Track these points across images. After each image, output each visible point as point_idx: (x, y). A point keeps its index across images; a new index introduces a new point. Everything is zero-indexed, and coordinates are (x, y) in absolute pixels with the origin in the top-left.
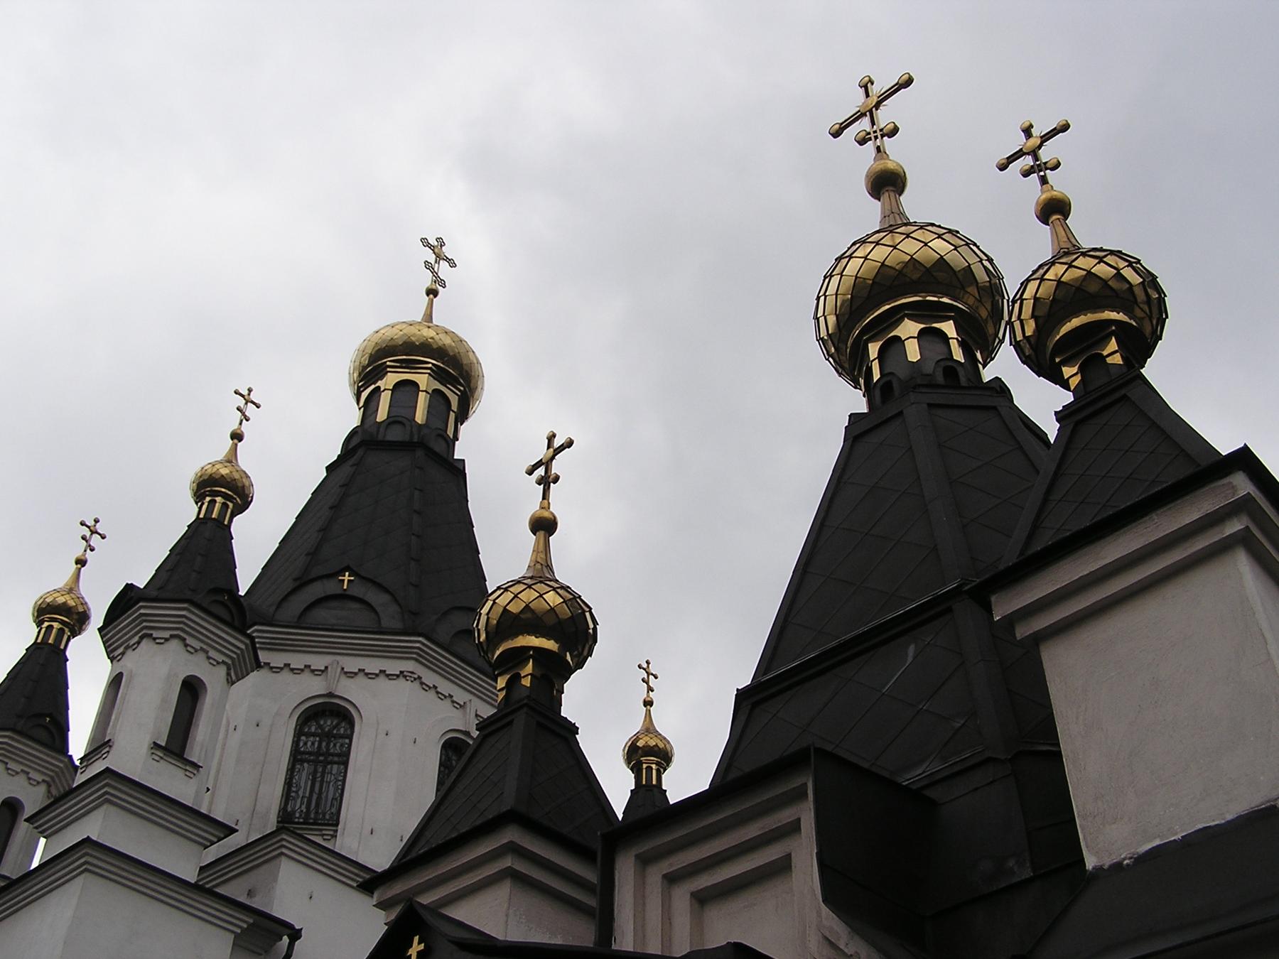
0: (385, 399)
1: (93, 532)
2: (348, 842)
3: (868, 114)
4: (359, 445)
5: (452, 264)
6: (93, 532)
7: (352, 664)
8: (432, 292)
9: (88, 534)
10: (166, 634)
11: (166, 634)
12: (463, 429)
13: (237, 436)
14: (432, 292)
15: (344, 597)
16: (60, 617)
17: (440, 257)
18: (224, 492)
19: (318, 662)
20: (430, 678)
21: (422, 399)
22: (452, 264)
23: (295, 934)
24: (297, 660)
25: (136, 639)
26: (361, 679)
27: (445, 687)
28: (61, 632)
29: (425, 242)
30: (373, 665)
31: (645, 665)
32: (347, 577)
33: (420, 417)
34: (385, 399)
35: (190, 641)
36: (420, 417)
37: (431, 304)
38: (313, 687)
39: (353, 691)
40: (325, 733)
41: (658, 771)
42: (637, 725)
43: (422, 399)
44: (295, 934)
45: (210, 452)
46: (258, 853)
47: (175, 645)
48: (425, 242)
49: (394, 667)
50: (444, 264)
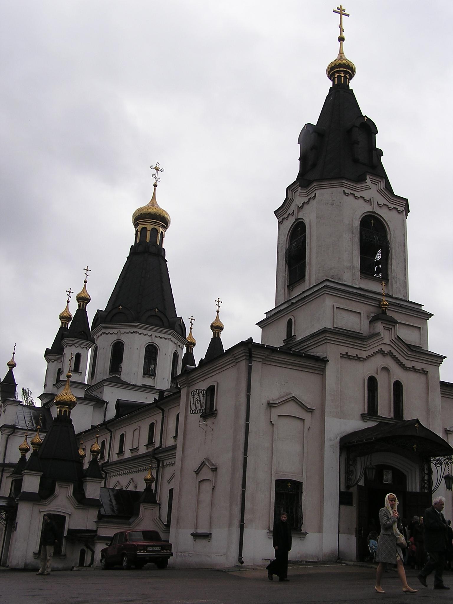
0: (139, 233)
1: (70, 292)
2: (124, 377)
4: (134, 250)
5: (163, 170)
6: (70, 292)
7: (123, 330)
8: (155, 186)
9: (68, 293)
12: (167, 234)
13: (86, 282)
14: (155, 186)
15: (120, 312)
17: (157, 169)
18: (83, 300)
19: (116, 331)
20: (141, 331)
21: (149, 233)
22: (163, 170)
23: (107, 403)
24: (111, 331)
27: (145, 332)
28: (66, 323)
29: (152, 167)
30: (127, 330)
31: (217, 300)
33: (148, 240)
34: (139, 233)
36: (148, 240)
37: (155, 189)
38: (114, 338)
39: (124, 338)
40: (118, 350)
41: (218, 333)
42: (213, 320)
43: (149, 233)
44: (107, 403)
45: (77, 290)
46: (100, 385)
47: (73, 346)
48: (152, 167)
50: (159, 172)
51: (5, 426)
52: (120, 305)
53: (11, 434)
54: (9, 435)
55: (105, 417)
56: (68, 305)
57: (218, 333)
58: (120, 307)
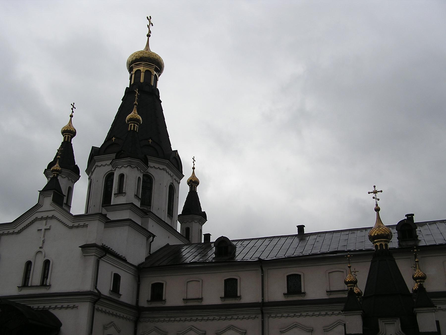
3: (375, 192)
10: (134, 166)
11: (134, 166)
14: (149, 36)
16: (69, 133)
20: (168, 170)
23: (154, 236)
25: (126, 165)
26: (154, 169)
27: (170, 172)
28: (68, 137)
30: (157, 166)
32: (150, 141)
35: (139, 168)
44: (154, 236)
47: (136, 169)
49: (162, 167)
51: (94, 245)
52: (150, 138)
53: (102, 257)
54: (100, 258)
55: (150, 251)
56: (71, 119)
57: (194, 187)
58: (114, 138)
